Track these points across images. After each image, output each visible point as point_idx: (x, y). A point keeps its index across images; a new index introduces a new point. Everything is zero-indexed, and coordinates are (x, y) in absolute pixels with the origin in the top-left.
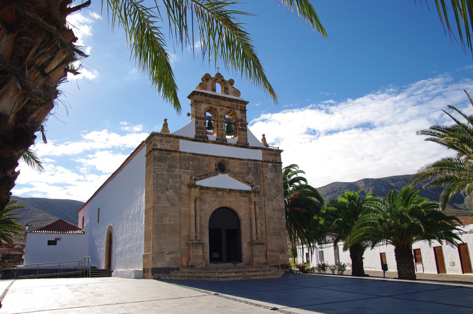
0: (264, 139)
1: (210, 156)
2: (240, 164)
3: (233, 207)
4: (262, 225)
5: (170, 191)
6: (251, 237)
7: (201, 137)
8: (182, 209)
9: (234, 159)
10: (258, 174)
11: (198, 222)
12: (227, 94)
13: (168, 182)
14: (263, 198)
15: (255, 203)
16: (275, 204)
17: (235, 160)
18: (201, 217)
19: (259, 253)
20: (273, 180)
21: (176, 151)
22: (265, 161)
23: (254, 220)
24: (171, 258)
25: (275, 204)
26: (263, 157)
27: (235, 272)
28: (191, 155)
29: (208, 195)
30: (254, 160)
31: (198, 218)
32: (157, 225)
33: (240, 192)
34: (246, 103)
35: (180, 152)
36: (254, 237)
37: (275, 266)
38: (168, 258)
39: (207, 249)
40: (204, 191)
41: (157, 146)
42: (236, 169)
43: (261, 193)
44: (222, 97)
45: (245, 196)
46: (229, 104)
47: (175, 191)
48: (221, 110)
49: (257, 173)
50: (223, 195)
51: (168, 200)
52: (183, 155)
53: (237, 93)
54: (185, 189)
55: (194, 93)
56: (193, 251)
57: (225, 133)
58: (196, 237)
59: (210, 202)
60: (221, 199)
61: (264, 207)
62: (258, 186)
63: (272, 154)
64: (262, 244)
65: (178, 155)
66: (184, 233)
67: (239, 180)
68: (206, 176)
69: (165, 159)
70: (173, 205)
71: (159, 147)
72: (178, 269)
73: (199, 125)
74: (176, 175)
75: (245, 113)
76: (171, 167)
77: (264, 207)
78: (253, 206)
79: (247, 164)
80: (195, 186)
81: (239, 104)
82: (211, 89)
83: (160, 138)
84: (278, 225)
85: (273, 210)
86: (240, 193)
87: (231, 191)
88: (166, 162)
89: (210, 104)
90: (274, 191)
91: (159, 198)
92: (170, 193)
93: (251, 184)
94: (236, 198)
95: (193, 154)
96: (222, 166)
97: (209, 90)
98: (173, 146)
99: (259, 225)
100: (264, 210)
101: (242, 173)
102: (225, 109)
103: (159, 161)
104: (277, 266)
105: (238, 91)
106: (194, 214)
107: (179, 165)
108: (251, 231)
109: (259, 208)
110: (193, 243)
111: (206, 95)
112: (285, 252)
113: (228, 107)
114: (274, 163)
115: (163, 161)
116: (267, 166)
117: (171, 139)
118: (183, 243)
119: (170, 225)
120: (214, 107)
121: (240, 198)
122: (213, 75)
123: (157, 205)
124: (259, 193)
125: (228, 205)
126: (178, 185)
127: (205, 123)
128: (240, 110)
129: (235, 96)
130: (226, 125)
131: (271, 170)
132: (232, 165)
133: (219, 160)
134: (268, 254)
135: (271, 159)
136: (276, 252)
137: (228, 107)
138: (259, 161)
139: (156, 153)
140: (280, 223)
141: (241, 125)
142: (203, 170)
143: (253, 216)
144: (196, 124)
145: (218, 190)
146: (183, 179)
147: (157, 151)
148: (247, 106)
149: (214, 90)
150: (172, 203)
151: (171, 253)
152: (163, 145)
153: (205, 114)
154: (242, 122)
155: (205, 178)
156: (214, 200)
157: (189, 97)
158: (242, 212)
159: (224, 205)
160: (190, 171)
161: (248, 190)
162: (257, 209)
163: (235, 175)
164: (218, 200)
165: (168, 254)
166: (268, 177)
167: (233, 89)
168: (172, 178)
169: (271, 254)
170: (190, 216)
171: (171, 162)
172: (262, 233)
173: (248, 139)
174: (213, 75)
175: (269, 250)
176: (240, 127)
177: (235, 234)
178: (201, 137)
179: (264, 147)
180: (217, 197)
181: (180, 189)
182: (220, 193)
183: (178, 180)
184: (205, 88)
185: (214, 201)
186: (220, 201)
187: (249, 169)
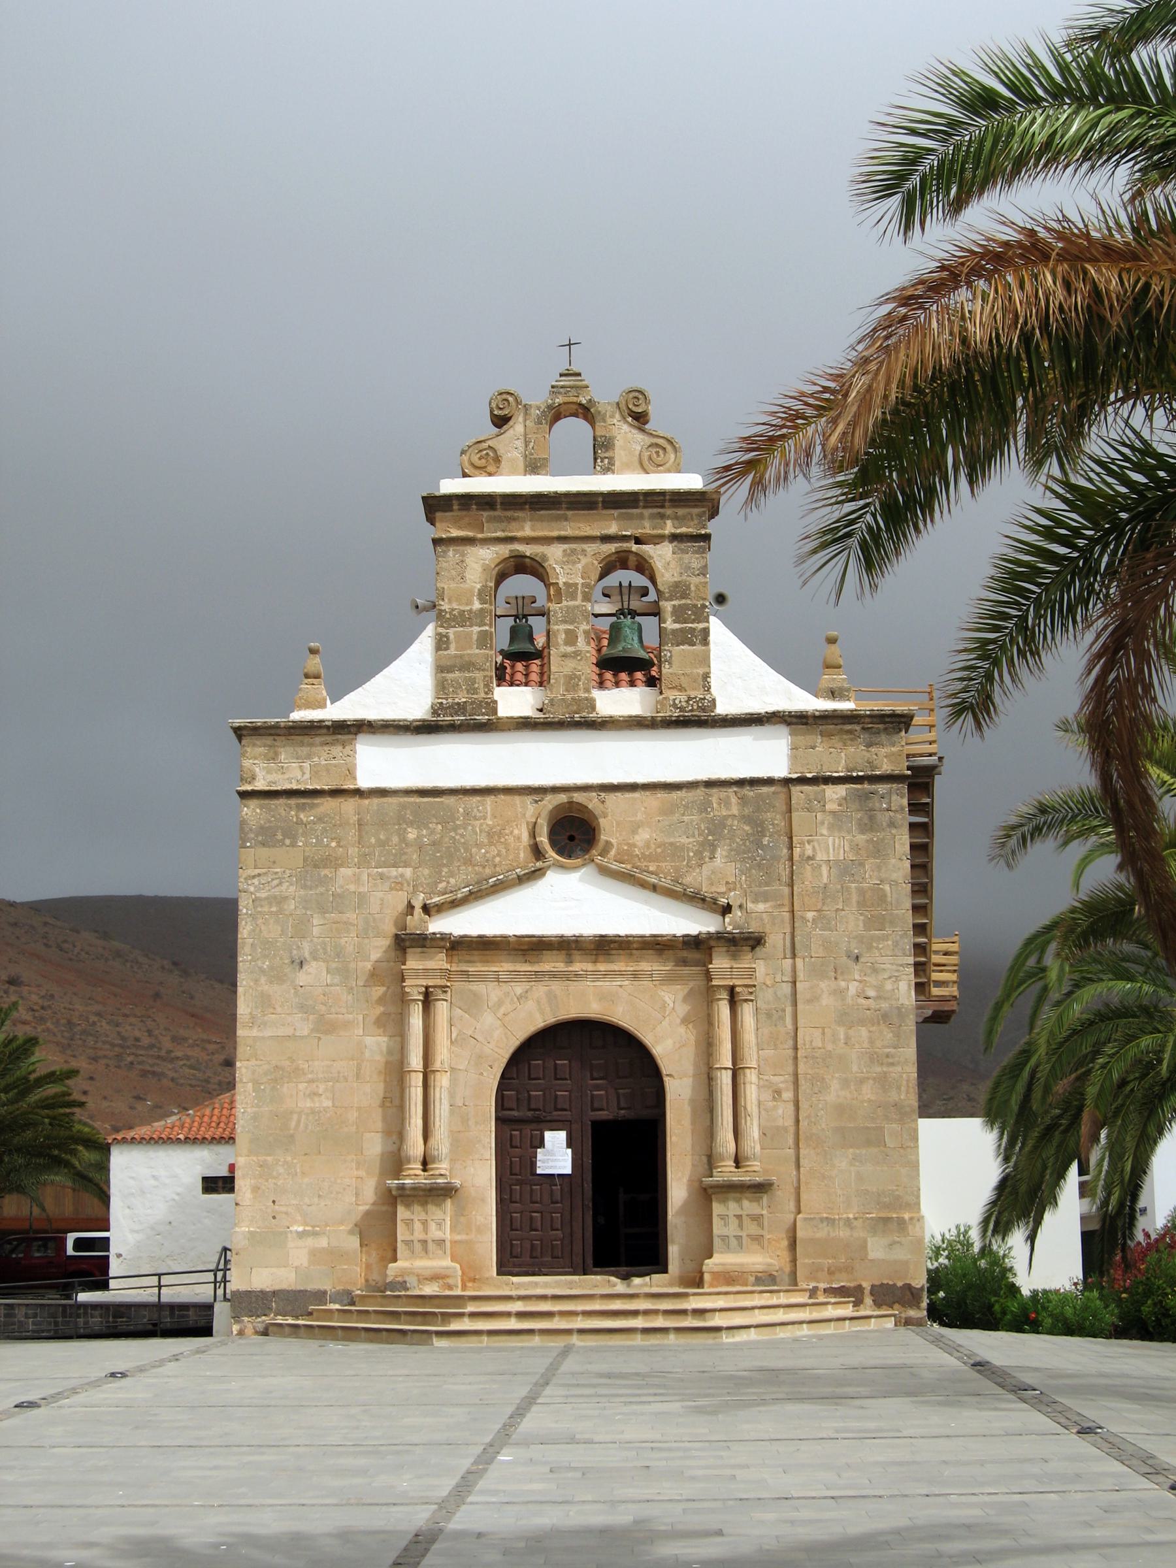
2: (667, 811)
3: (621, 1016)
4: (778, 1092)
5: (312, 967)
8: (369, 1040)
9: (633, 787)
10: (762, 847)
12: (608, 470)
13: (301, 930)
14: (788, 962)
15: (732, 990)
16: (853, 988)
17: (636, 795)
20: (845, 870)
21: (336, 793)
22: (802, 781)
23: (725, 1079)
24: (314, 1253)
26: (794, 759)
30: (741, 783)
31: (442, 1082)
32: (255, 1117)
33: (657, 945)
35: (358, 793)
37: (842, 1292)
39: (487, 1212)
43: (776, 940)
45: (684, 962)
47: (334, 965)
49: (760, 845)
51: (304, 1008)
52: (376, 801)
57: (589, 670)
59: (500, 1003)
60: (556, 986)
61: (789, 1010)
62: (761, 907)
65: (349, 806)
67: (654, 888)
69: (290, 834)
73: (452, 651)
74: (340, 896)
79: (705, 807)
80: (424, 942)
81: (669, 512)
84: (868, 1092)
85: (845, 1018)
87: (604, 947)
88: (293, 845)
90: (852, 922)
91: (265, 1001)
92: (314, 975)
96: (573, 831)
97: (513, 472)
98: (327, 769)
101: (676, 851)
102: (591, 548)
104: (853, 1294)
105: (670, 442)
107: (353, 851)
109: (766, 1016)
113: (606, 539)
117: (318, 740)
119: (313, 1111)
123: (255, 1032)
125: (593, 1009)
126: (349, 942)
128: (674, 538)
134: (800, 1234)
137: (606, 539)
138: (769, 781)
140: (883, 1081)
141: (679, 614)
142: (469, 861)
146: (375, 908)
154: (684, 596)
158: (669, 1041)
159: (572, 1011)
160: (408, 872)
161: (694, 932)
166: (820, 856)
168: (323, 911)
171: (319, 842)
173: (714, 681)
178: (460, 708)
180: (538, 976)
187: (717, 828)
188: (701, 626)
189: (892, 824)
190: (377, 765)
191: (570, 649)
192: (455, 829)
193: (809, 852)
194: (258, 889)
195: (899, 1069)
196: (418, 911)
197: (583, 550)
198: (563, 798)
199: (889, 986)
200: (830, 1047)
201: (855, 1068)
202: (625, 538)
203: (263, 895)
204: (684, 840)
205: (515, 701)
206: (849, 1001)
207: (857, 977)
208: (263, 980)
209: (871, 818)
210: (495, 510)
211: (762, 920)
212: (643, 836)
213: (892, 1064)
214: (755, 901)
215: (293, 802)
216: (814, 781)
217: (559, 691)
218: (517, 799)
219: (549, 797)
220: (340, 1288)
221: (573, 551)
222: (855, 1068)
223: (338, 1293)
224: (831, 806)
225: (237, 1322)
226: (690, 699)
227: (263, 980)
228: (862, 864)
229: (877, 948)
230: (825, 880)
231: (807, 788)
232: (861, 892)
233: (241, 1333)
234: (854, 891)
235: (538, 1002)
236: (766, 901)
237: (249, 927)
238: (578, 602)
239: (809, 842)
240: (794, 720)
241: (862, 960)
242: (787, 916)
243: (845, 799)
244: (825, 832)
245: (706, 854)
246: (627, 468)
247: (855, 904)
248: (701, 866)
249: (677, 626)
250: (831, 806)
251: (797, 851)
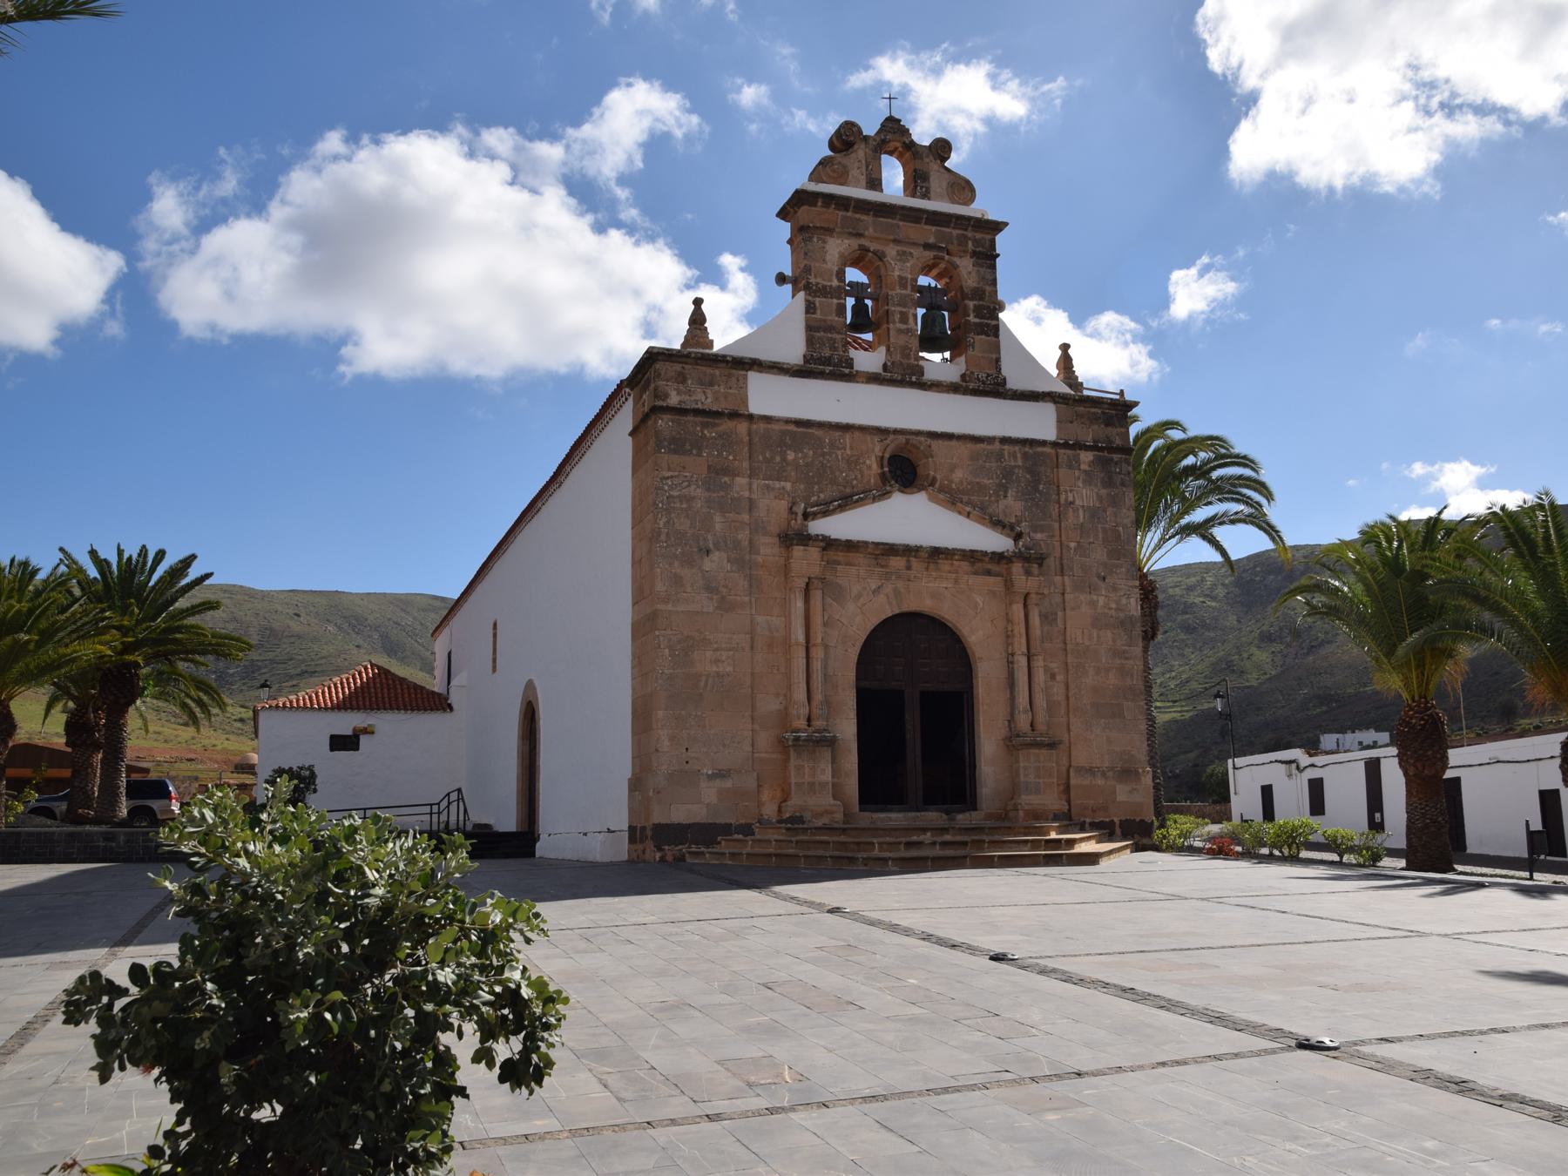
0: (1066, 362)
1: (863, 429)
2: (974, 457)
3: (946, 611)
4: (1053, 676)
5: (716, 555)
6: (1011, 720)
7: (824, 362)
8: (760, 619)
11: (817, 665)
12: (926, 195)
14: (1058, 579)
15: (1027, 596)
16: (1101, 601)
17: (954, 443)
18: (826, 647)
19: (1038, 776)
20: (1094, 514)
21: (734, 415)
22: (1066, 445)
23: (1023, 661)
25: (1101, 601)
26: (1059, 429)
27: (944, 844)
28: (792, 427)
29: (853, 570)
31: (818, 653)
33: (972, 556)
34: (998, 227)
35: (751, 417)
36: (1023, 721)
38: (710, 793)
39: (851, 761)
40: (840, 556)
41: (666, 396)
42: (958, 475)
43: (1051, 562)
44: (903, 208)
45: (989, 573)
46: (930, 233)
48: (903, 256)
49: (1037, 490)
50: (909, 568)
51: (710, 589)
52: (762, 426)
53: (963, 189)
54: (768, 550)
55: (800, 198)
56: (799, 768)
57: (915, 343)
58: (809, 720)
59: (859, 596)
60: (900, 585)
62: (1039, 536)
63: (1094, 419)
64: (1052, 745)
65: (742, 427)
66: (770, 704)
67: (968, 515)
68: (846, 502)
70: (725, 606)
71: (674, 400)
72: (747, 830)
73: (818, 315)
75: (993, 267)
76: (719, 471)
77: (1060, 614)
78: (1018, 609)
79: (1000, 457)
80: (806, 539)
82: (863, 179)
83: (678, 367)
84: (1113, 679)
86: (972, 564)
87: (937, 554)
88: (699, 455)
89: (860, 235)
90: (1099, 554)
91: (677, 581)
92: (715, 563)
93: (1012, 528)
94: (956, 581)
95: (799, 423)
96: (905, 465)
99: (1040, 677)
100: (1060, 621)
103: (675, 452)
105: (968, 183)
106: (800, 636)
107: (746, 464)
108: (1013, 699)
109: (1045, 617)
110: (797, 739)
111: (843, 203)
112: (1137, 772)
115: (689, 453)
116: (1073, 464)
118: (765, 739)
119: (718, 674)
120: (873, 246)
121: (973, 580)
122: (870, 128)
123: (669, 607)
124: (1041, 560)
125: (926, 605)
126: (744, 536)
127: (841, 309)
128: (974, 254)
129: (953, 202)
130: (921, 312)
131: (1089, 478)
132: (940, 463)
133: (893, 444)
134: (1073, 781)
135: (1088, 435)
136: (1104, 774)
137: (927, 246)
138: (1043, 443)
139: (663, 423)
141: (978, 311)
143: (1020, 645)
144: (807, 312)
145: (890, 550)
147: (666, 417)
148: (1001, 240)
149: (875, 183)
150: (723, 598)
151: (721, 775)
152: (690, 393)
153: (841, 275)
154: (982, 298)
155: (841, 508)
156: (874, 586)
157: (783, 214)
159: (911, 605)
160: (788, 486)
161: (999, 550)
162: (1035, 620)
163: (952, 498)
164: (888, 588)
165: (711, 777)
167: (947, 175)
169: (1086, 782)
170: (787, 645)
171: (720, 454)
172: (1051, 707)
174: (870, 128)
175: (1080, 770)
176: (972, 319)
177: (952, 712)
178: (827, 361)
179: (1066, 390)
181: (752, 548)
182: (897, 562)
183: (746, 517)
184: (841, 179)
185: (876, 591)
186: (896, 591)
187: (1008, 473)
189: (1123, 484)
190: (769, 398)
192: (823, 455)
194: (671, 488)
196: (800, 517)
198: (902, 439)
199: (1124, 601)
202: (940, 249)
203: (675, 493)
205: (868, 360)
208: (676, 564)
209: (1110, 478)
212: (958, 475)
215: (699, 419)
216: (1072, 447)
217: (898, 357)
218: (869, 438)
219: (892, 437)
220: (743, 821)
223: (741, 825)
224: (1084, 467)
225: (660, 849)
227: (676, 564)
232: (1105, 531)
233: (663, 859)
236: (1042, 531)
237: (664, 519)
238: (908, 291)
242: (1057, 544)
246: (940, 198)
250: (1084, 467)
251: (1063, 497)
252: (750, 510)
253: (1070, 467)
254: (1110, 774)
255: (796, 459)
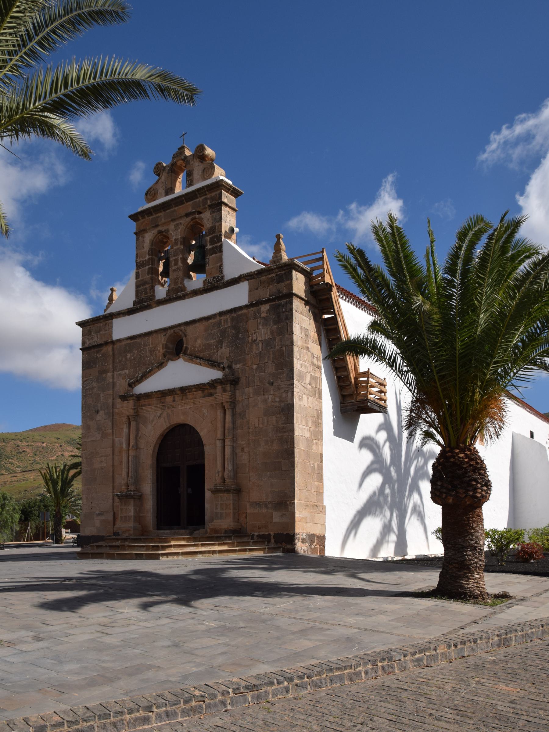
16: (270, 399)
17: (197, 325)
20: (268, 343)
26: (250, 295)
42: (199, 341)
43: (243, 380)
50: (174, 401)
59: (153, 421)
62: (238, 366)
79: (219, 324)
86: (203, 391)
87: (184, 390)
94: (194, 403)
114: (273, 300)
136: (266, 506)
138: (241, 308)
141: (212, 242)
156: (159, 414)
166: (259, 339)
171: (102, 364)
186: (168, 415)
188: (219, 244)
191: (176, 267)
193: (255, 338)
195: (287, 434)
197: (181, 223)
199: (284, 395)
200: (261, 426)
201: (270, 435)
203: (87, 387)
204: (212, 341)
206: (269, 404)
207: (272, 393)
208: (88, 420)
210: (152, 215)
211: (238, 372)
213: (285, 432)
214: (236, 364)
221: (177, 225)
222: (270, 435)
226: (214, 278)
227: (88, 420)
228: (275, 340)
229: (280, 378)
230: (260, 350)
231: (255, 309)
234: (271, 353)
235: (164, 418)
239: (255, 333)
240: (249, 278)
241: (274, 385)
243: (269, 310)
244: (261, 327)
245: (220, 346)
247: (271, 358)
248: (217, 351)
249: (211, 246)
250: (263, 315)
252: (113, 388)
253: (255, 318)
254: (270, 506)
255: (131, 356)
